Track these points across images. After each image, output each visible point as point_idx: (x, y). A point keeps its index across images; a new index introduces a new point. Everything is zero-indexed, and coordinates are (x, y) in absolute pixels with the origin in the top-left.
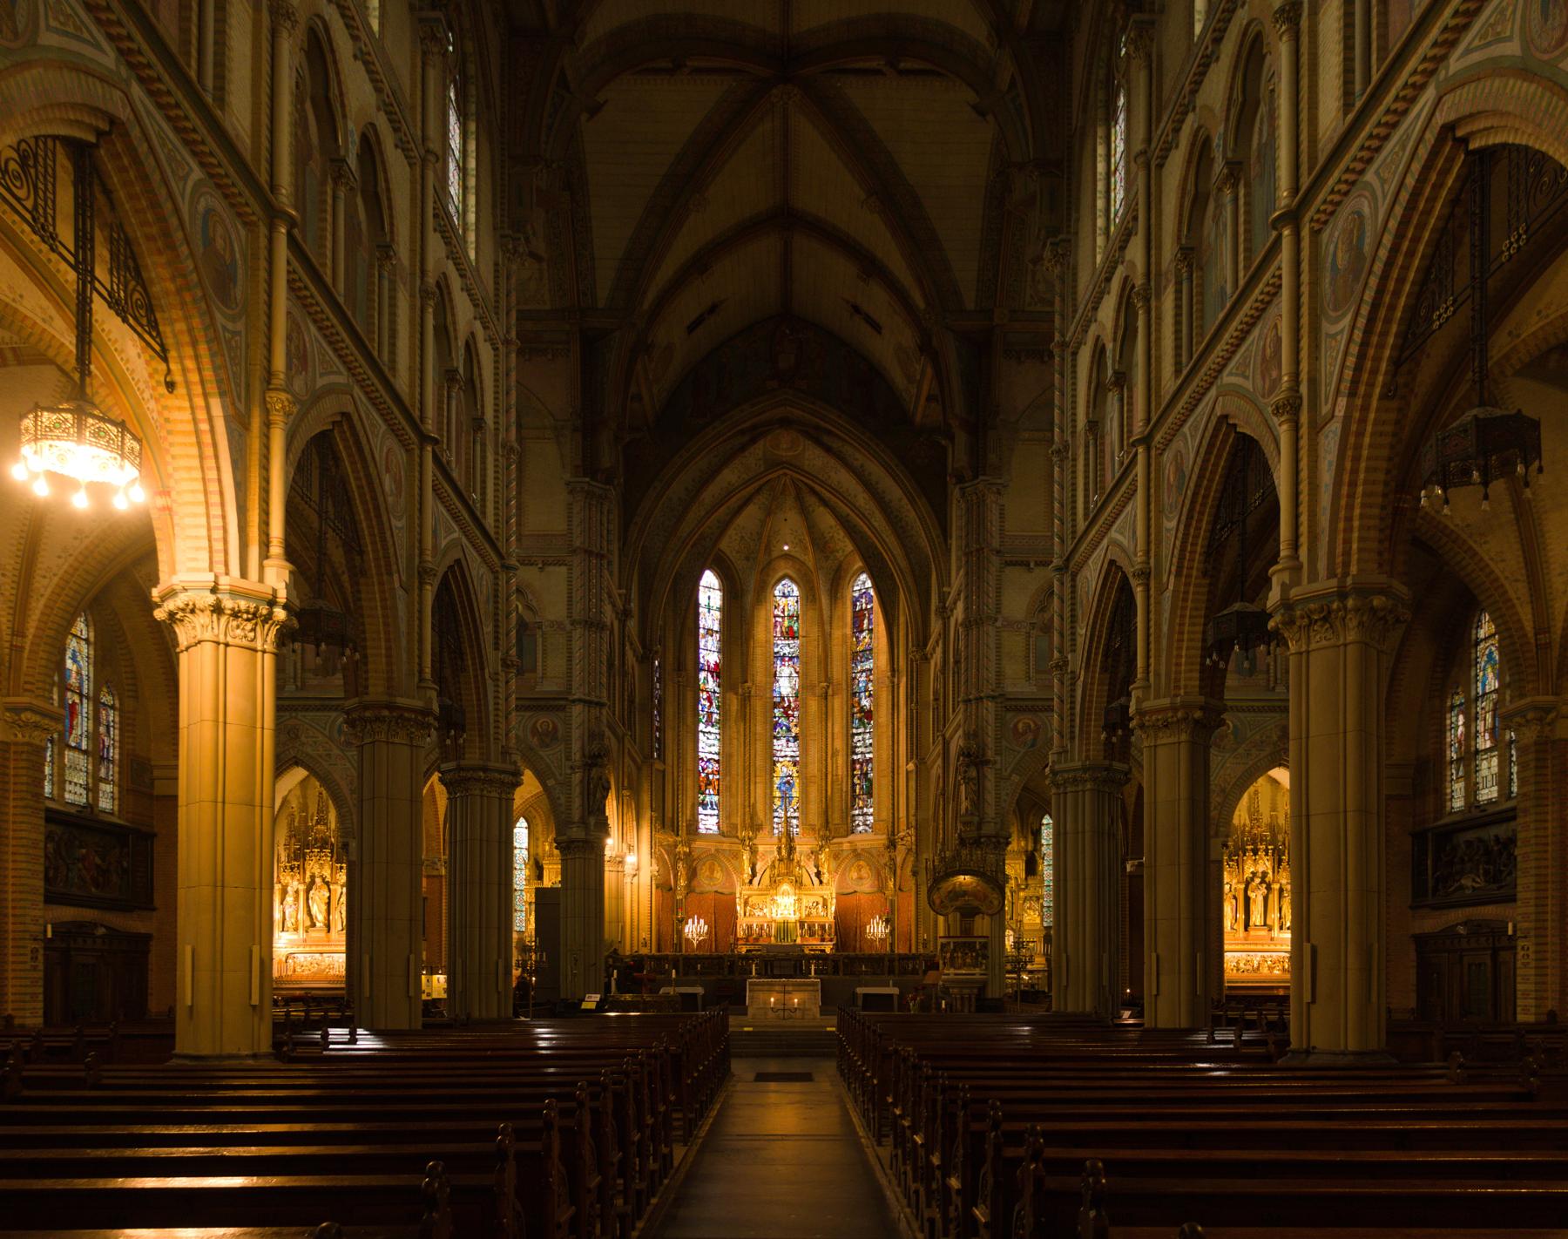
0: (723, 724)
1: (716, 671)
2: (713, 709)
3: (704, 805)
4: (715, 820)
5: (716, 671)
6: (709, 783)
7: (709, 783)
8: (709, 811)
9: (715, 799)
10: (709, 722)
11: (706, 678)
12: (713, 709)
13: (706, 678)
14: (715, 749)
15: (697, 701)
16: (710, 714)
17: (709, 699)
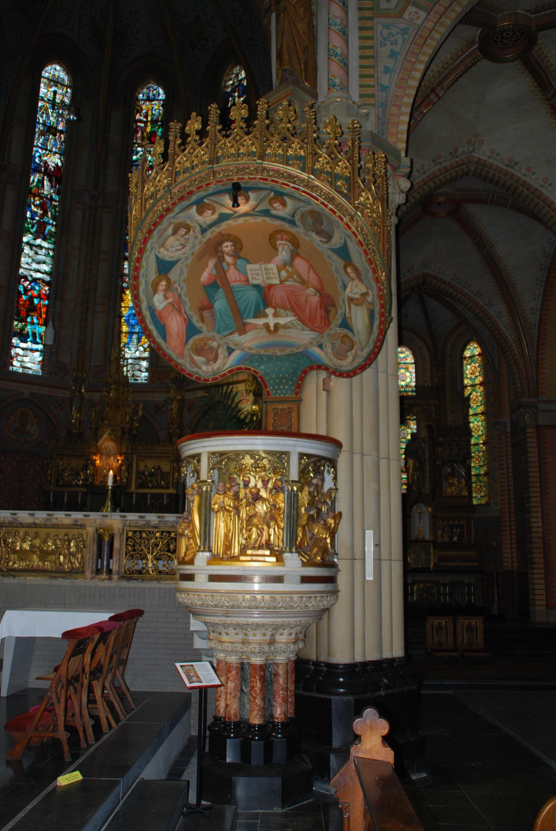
0: (61, 241)
1: (55, 175)
2: (49, 219)
3: (24, 338)
4: (38, 357)
5: (55, 175)
6: (32, 309)
7: (32, 309)
8: (29, 345)
9: (42, 329)
10: (40, 233)
11: (41, 182)
12: (49, 219)
13: (41, 182)
14: (45, 268)
15: (24, 206)
16: (42, 225)
17: (42, 206)
